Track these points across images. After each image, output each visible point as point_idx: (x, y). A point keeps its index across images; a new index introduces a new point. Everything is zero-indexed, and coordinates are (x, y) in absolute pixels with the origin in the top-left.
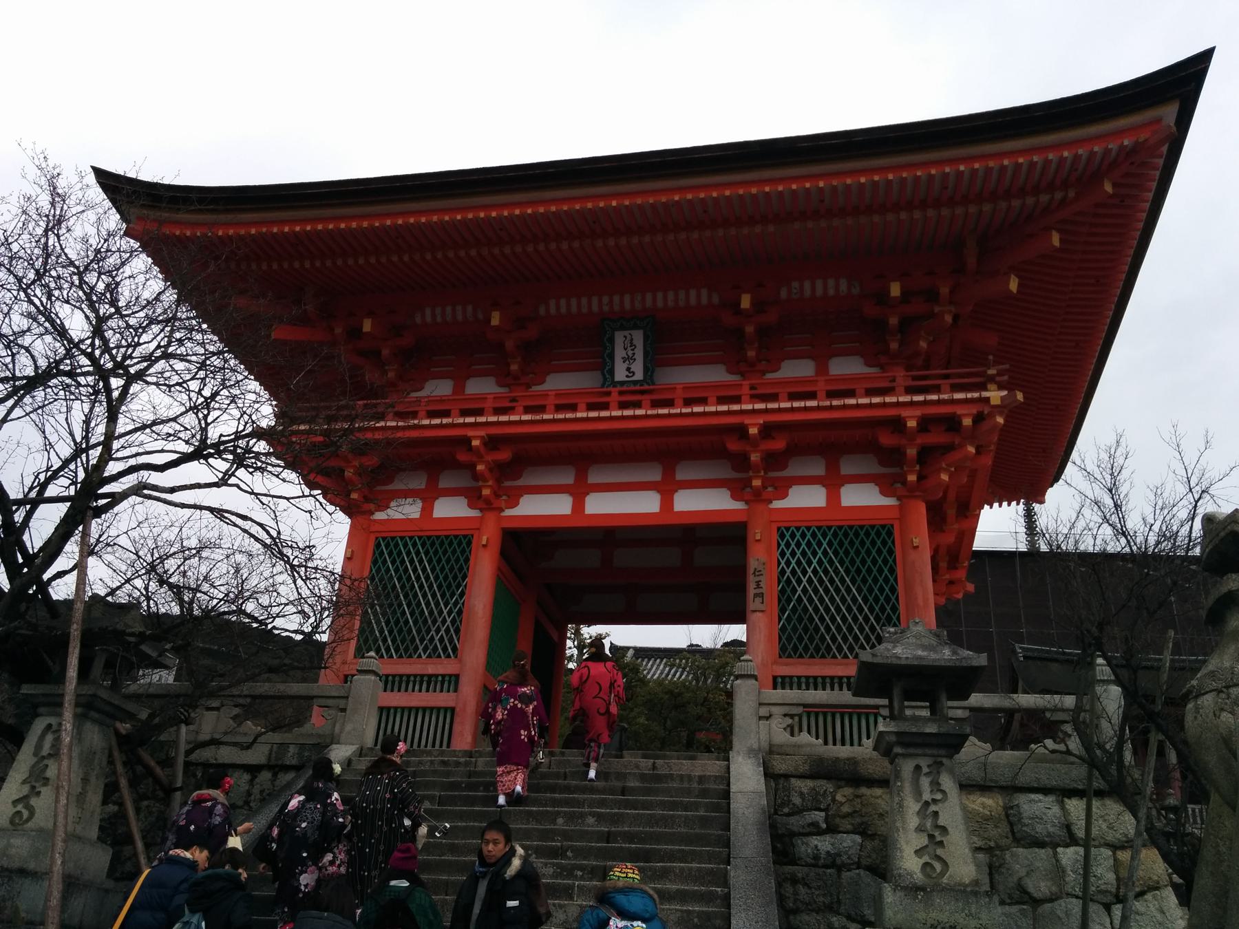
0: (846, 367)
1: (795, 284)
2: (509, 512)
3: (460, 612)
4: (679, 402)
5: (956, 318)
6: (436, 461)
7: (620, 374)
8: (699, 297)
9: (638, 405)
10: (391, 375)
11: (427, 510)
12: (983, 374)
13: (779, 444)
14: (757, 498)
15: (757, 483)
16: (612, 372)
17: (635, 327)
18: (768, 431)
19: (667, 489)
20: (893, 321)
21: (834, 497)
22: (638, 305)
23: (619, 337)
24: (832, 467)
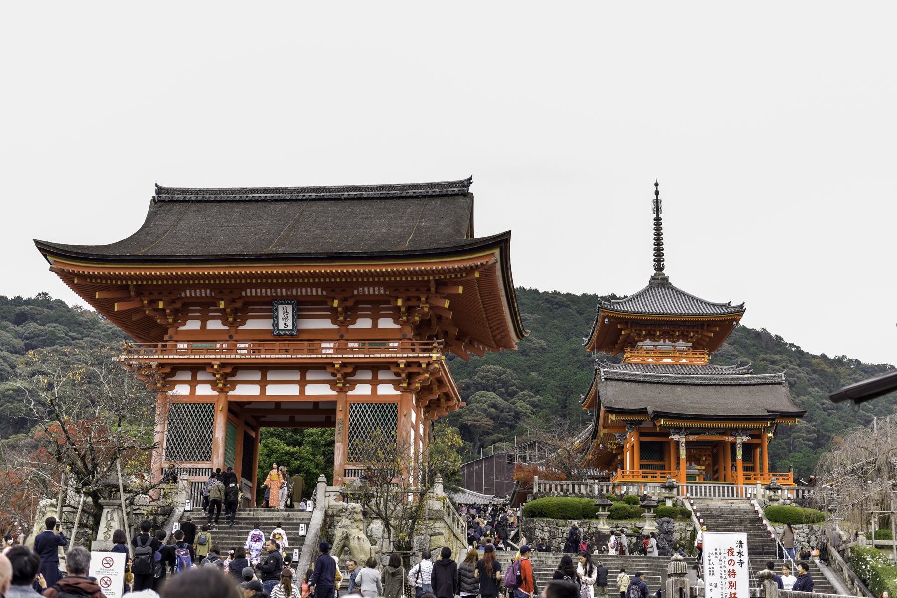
0: (386, 323)
1: (361, 289)
2: (231, 393)
3: (211, 440)
4: (306, 351)
5: (430, 308)
6: (195, 368)
7: (281, 326)
8: (317, 291)
9: (287, 351)
10: (170, 320)
11: (193, 391)
12: (431, 344)
13: (349, 370)
14: (342, 391)
15: (340, 385)
16: (277, 325)
17: (288, 304)
18: (344, 365)
19: (303, 383)
20: (403, 309)
21: (374, 390)
22: (289, 293)
23: (280, 308)
24: (375, 376)
